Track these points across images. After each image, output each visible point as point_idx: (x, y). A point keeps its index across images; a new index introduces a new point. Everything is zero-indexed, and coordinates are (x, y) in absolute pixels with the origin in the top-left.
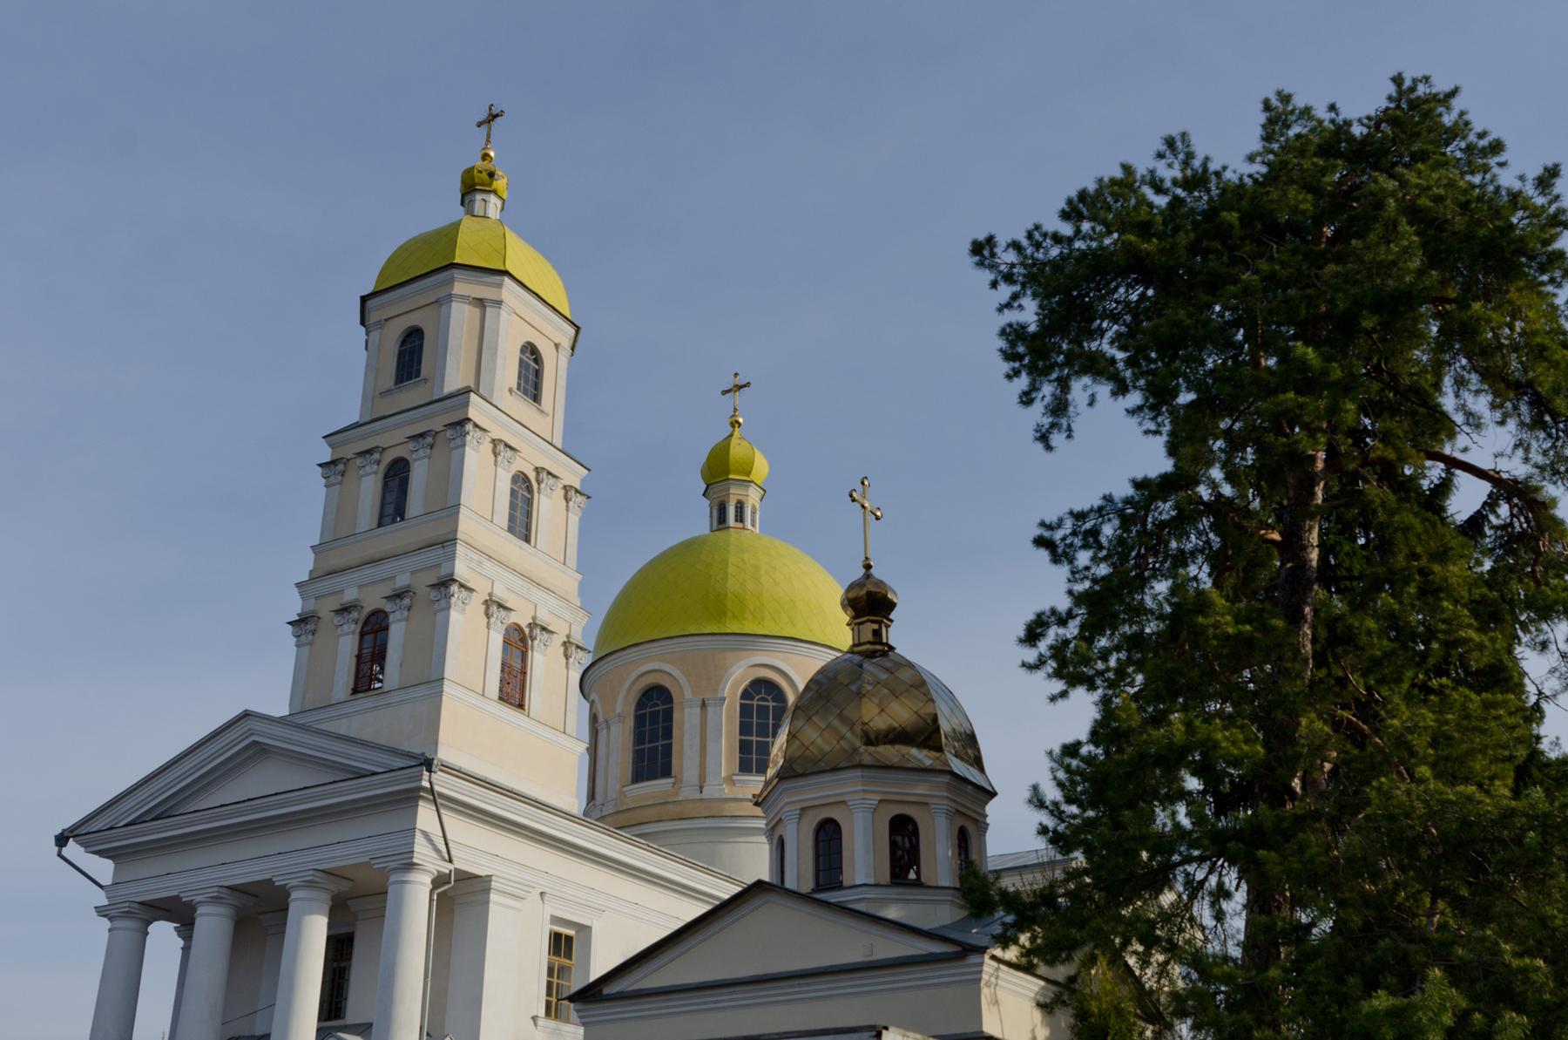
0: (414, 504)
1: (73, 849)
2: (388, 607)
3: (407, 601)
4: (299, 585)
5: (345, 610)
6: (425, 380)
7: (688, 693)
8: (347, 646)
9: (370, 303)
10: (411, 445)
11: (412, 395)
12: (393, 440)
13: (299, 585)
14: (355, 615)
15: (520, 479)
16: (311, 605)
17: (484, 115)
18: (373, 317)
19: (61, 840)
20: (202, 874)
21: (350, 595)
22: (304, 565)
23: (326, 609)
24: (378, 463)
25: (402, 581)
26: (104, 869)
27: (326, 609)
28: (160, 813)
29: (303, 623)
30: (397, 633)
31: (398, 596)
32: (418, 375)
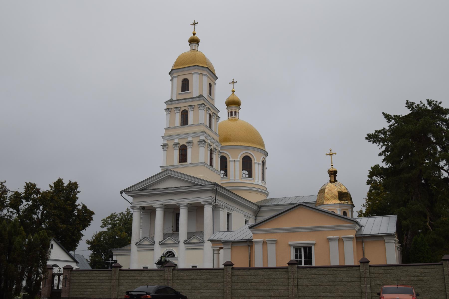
1: (124, 194)
2: (187, 145)
3: (192, 144)
4: (162, 137)
5: (175, 144)
6: (190, 92)
7: (231, 159)
8: (176, 153)
9: (173, 71)
10: (189, 107)
11: (186, 95)
12: (184, 106)
13: (162, 137)
14: (178, 145)
15: (210, 115)
16: (165, 142)
17: (193, 22)
18: (175, 75)
19: (121, 192)
20: (157, 202)
21: (176, 141)
22: (163, 133)
23: (170, 144)
24: (180, 110)
25: (190, 139)
26: (130, 199)
27: (170, 144)
28: (144, 189)
30: (189, 152)
31: (189, 143)
32: (188, 90)
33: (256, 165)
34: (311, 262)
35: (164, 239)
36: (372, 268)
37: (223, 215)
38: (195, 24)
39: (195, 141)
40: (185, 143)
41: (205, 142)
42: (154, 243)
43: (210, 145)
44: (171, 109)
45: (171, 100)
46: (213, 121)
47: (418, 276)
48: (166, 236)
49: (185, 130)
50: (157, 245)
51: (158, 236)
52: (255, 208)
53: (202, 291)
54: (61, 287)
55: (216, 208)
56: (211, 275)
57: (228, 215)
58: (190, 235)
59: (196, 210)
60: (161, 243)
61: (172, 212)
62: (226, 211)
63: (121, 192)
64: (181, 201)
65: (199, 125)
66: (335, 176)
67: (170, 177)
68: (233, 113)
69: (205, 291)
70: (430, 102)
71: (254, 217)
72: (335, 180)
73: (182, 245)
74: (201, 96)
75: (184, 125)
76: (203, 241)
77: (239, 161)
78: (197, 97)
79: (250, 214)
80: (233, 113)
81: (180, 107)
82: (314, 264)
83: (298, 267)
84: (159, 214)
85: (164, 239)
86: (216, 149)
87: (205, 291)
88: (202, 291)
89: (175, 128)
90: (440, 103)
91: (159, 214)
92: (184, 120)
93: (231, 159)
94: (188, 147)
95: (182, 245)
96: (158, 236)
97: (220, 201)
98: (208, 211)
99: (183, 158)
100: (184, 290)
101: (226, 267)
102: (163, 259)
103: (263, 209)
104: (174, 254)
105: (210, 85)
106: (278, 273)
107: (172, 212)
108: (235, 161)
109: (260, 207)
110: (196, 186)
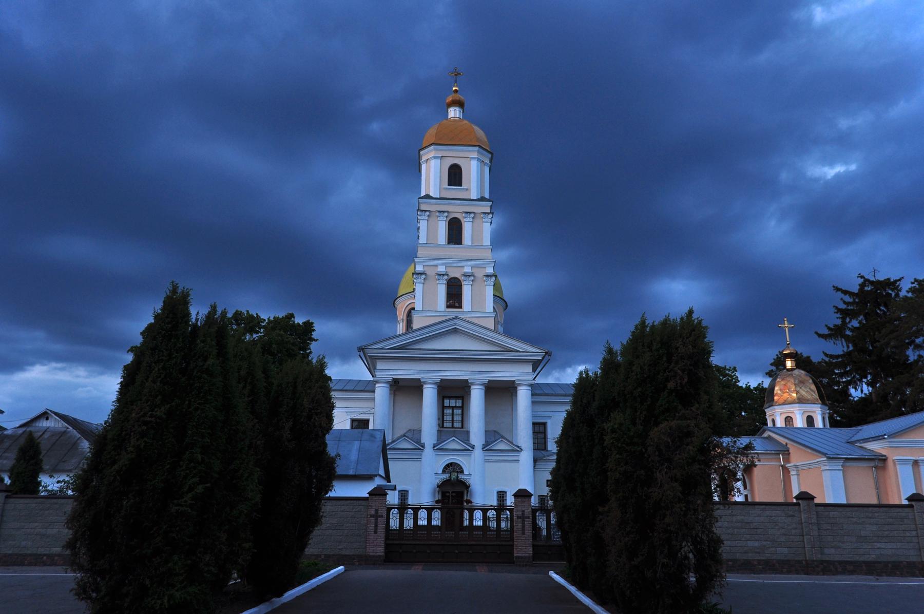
2: (462, 278)
8: (442, 290)
11: (455, 192)
14: (446, 277)
21: (442, 269)
25: (468, 270)
30: (467, 291)
31: (467, 276)
39: (479, 274)
40: (458, 275)
49: (454, 251)
50: (428, 452)
53: (879, 545)
56: (891, 517)
58: (491, 436)
60: (438, 448)
61: (453, 393)
64: (478, 376)
67: (455, 331)
69: (882, 545)
73: (478, 453)
81: (448, 212)
84: (430, 394)
87: (882, 545)
88: (879, 545)
89: (437, 245)
94: (463, 283)
95: (478, 453)
96: (429, 434)
100: (843, 542)
104: (461, 468)
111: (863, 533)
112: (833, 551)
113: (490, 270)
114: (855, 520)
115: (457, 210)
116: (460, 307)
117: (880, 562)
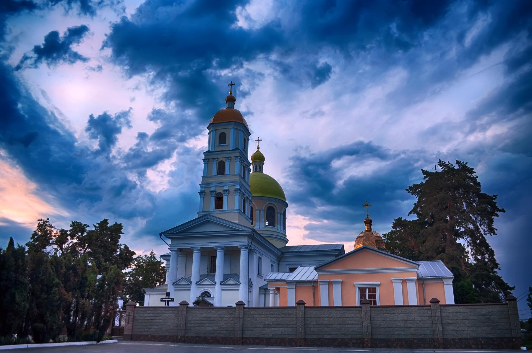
0: (227, 172)
2: (223, 193)
5: (212, 192)
8: (213, 200)
15: (244, 166)
19: (161, 234)
20: (196, 245)
21: (213, 189)
25: (226, 188)
27: (208, 191)
29: (201, 193)
31: (225, 191)
33: (279, 215)
34: (375, 302)
35: (200, 280)
36: (442, 308)
37: (255, 257)
38: (231, 85)
39: (232, 189)
41: (241, 191)
42: (191, 283)
43: (244, 194)
44: (208, 159)
45: (209, 151)
46: (246, 172)
47: (486, 315)
48: (202, 277)
50: (193, 286)
51: (194, 278)
52: (279, 253)
53: (274, 329)
54: (123, 324)
55: (250, 252)
56: (283, 314)
57: (260, 258)
58: (226, 277)
59: (232, 254)
60: (198, 284)
62: (258, 255)
63: (161, 234)
65: (234, 175)
66: (371, 225)
68: (258, 168)
69: (277, 329)
70: (458, 163)
71: (278, 262)
72: (371, 229)
73: (218, 286)
74: (237, 149)
75: (220, 175)
76: (239, 282)
77: (264, 211)
78: (233, 150)
79: (274, 258)
80: (258, 168)
81: (218, 158)
82: (378, 304)
83: (371, 307)
84: (196, 256)
85: (200, 280)
86: (248, 198)
87: (277, 329)
88: (274, 329)
89: (211, 176)
90: (466, 163)
91: (196, 256)
92: (221, 171)
93: (257, 208)
95: (218, 286)
96: (194, 276)
97: (255, 246)
98: (243, 254)
99: (219, 204)
100: (255, 328)
101: (299, 306)
102: (201, 299)
103: (286, 255)
105: (245, 139)
106: (351, 312)
107: (209, 256)
108: (260, 211)
109: (283, 253)
110: (232, 232)
111: (267, 323)
112: (249, 332)
113: (238, 187)
114: (263, 315)
115: (222, 157)
116: (222, 208)
117: (274, 338)
